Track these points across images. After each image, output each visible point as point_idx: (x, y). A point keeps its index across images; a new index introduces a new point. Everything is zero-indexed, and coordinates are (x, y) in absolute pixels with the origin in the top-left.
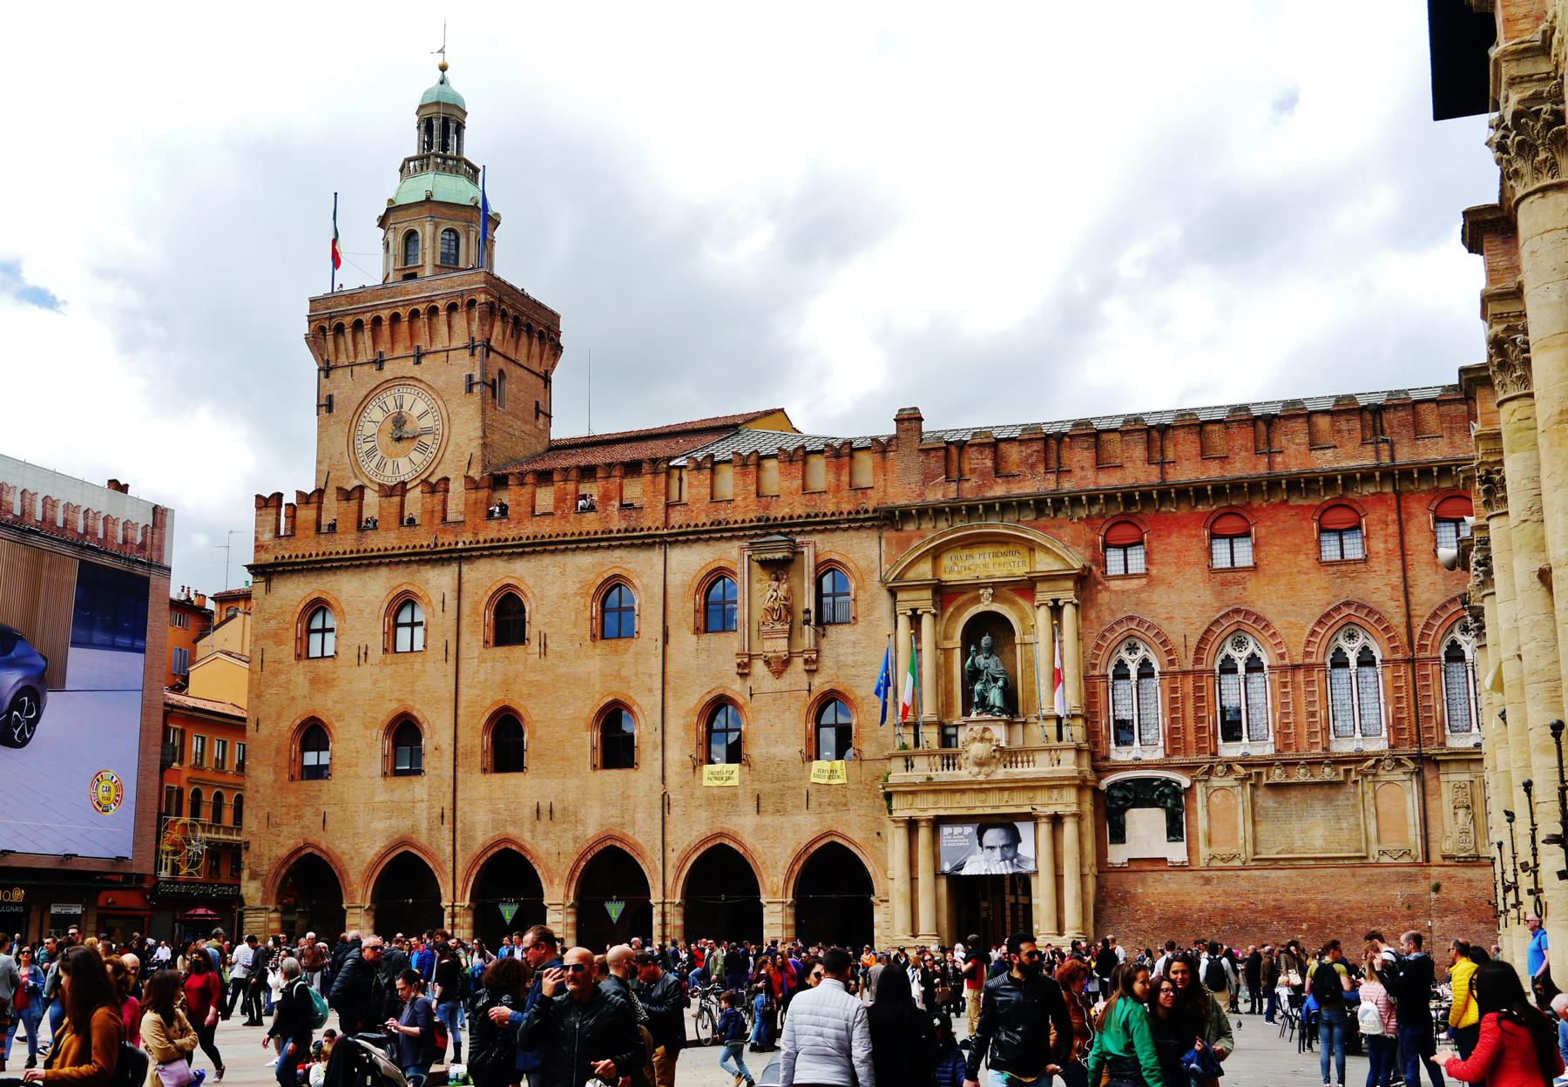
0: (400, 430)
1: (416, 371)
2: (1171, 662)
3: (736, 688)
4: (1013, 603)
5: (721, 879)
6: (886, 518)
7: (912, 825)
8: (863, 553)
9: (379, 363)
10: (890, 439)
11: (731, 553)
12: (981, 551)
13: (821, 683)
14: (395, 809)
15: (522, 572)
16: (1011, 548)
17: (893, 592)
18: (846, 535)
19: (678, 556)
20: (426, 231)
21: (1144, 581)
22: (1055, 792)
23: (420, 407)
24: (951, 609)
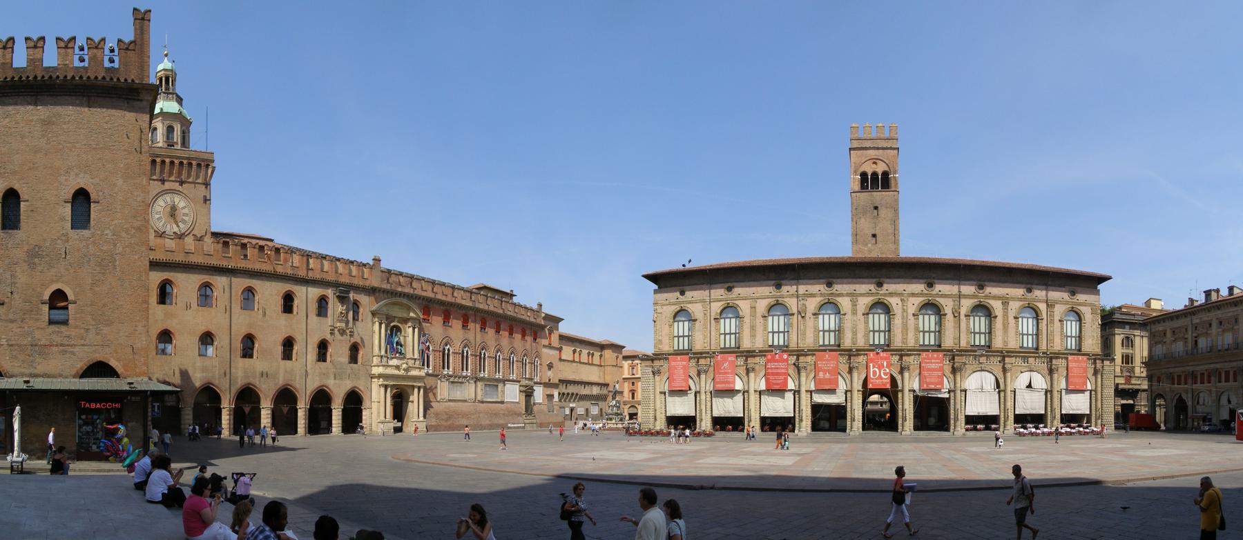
0: (173, 212)
1: (180, 188)
3: (328, 337)
5: (321, 399)
8: (364, 300)
9: (163, 181)
11: (330, 293)
13: (353, 340)
14: (204, 369)
15: (255, 283)
19: (310, 289)
20: (178, 128)
23: (182, 204)
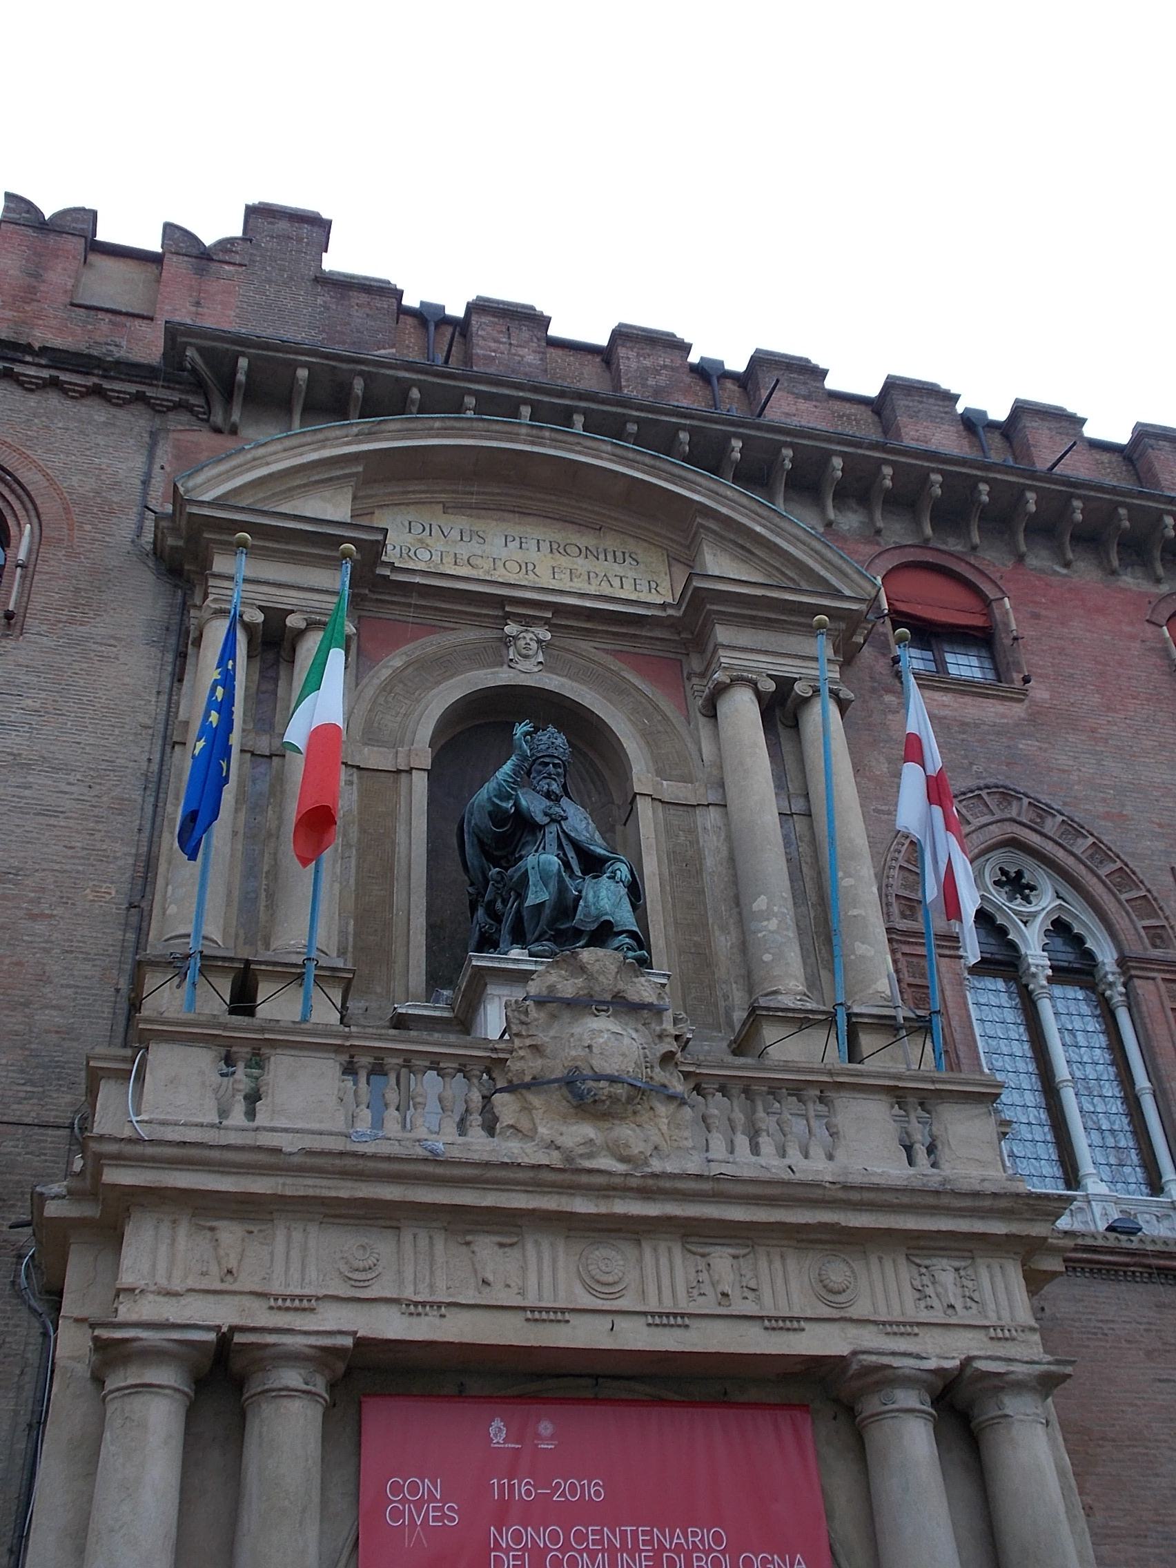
2: (1157, 936)
4: (617, 690)
6: (199, 386)
7: (222, 1377)
10: (226, 244)
12: (515, 529)
16: (610, 542)
17: (182, 556)
18: (32, 400)
21: (1018, 710)
22: (945, 1272)
24: (397, 661)
